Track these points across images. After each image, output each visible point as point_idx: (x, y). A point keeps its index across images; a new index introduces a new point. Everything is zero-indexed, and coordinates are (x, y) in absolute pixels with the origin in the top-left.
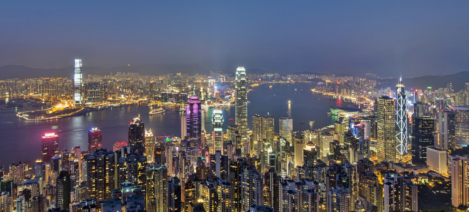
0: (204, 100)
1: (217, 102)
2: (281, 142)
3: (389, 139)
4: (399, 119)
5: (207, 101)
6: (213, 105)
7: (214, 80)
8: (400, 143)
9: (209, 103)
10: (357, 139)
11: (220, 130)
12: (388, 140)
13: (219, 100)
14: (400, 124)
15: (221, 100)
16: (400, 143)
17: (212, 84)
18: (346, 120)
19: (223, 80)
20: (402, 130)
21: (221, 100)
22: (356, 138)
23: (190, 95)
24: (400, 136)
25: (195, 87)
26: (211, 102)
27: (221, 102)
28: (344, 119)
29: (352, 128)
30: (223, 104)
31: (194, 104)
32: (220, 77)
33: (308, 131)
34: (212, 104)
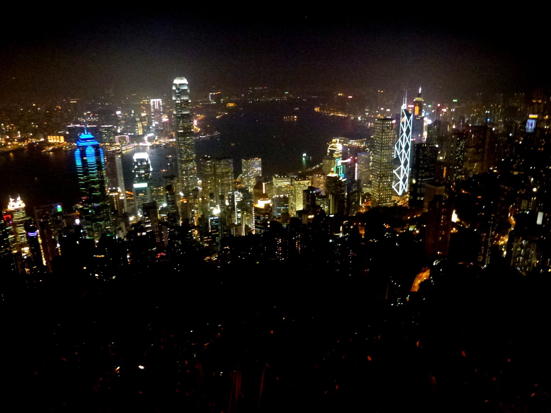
0: (143, 135)
1: (165, 136)
2: (236, 196)
3: (385, 177)
4: (401, 148)
6: (157, 143)
7: (158, 100)
8: (399, 180)
9: (150, 140)
10: (343, 180)
11: (144, 185)
12: (384, 178)
13: (170, 132)
14: (401, 155)
16: (399, 180)
17: (157, 107)
18: (338, 154)
20: (402, 162)
21: (172, 133)
22: (341, 181)
23: (121, 128)
24: (400, 169)
25: (133, 113)
26: (156, 137)
28: (335, 153)
29: (338, 165)
33: (277, 175)
34: (157, 141)
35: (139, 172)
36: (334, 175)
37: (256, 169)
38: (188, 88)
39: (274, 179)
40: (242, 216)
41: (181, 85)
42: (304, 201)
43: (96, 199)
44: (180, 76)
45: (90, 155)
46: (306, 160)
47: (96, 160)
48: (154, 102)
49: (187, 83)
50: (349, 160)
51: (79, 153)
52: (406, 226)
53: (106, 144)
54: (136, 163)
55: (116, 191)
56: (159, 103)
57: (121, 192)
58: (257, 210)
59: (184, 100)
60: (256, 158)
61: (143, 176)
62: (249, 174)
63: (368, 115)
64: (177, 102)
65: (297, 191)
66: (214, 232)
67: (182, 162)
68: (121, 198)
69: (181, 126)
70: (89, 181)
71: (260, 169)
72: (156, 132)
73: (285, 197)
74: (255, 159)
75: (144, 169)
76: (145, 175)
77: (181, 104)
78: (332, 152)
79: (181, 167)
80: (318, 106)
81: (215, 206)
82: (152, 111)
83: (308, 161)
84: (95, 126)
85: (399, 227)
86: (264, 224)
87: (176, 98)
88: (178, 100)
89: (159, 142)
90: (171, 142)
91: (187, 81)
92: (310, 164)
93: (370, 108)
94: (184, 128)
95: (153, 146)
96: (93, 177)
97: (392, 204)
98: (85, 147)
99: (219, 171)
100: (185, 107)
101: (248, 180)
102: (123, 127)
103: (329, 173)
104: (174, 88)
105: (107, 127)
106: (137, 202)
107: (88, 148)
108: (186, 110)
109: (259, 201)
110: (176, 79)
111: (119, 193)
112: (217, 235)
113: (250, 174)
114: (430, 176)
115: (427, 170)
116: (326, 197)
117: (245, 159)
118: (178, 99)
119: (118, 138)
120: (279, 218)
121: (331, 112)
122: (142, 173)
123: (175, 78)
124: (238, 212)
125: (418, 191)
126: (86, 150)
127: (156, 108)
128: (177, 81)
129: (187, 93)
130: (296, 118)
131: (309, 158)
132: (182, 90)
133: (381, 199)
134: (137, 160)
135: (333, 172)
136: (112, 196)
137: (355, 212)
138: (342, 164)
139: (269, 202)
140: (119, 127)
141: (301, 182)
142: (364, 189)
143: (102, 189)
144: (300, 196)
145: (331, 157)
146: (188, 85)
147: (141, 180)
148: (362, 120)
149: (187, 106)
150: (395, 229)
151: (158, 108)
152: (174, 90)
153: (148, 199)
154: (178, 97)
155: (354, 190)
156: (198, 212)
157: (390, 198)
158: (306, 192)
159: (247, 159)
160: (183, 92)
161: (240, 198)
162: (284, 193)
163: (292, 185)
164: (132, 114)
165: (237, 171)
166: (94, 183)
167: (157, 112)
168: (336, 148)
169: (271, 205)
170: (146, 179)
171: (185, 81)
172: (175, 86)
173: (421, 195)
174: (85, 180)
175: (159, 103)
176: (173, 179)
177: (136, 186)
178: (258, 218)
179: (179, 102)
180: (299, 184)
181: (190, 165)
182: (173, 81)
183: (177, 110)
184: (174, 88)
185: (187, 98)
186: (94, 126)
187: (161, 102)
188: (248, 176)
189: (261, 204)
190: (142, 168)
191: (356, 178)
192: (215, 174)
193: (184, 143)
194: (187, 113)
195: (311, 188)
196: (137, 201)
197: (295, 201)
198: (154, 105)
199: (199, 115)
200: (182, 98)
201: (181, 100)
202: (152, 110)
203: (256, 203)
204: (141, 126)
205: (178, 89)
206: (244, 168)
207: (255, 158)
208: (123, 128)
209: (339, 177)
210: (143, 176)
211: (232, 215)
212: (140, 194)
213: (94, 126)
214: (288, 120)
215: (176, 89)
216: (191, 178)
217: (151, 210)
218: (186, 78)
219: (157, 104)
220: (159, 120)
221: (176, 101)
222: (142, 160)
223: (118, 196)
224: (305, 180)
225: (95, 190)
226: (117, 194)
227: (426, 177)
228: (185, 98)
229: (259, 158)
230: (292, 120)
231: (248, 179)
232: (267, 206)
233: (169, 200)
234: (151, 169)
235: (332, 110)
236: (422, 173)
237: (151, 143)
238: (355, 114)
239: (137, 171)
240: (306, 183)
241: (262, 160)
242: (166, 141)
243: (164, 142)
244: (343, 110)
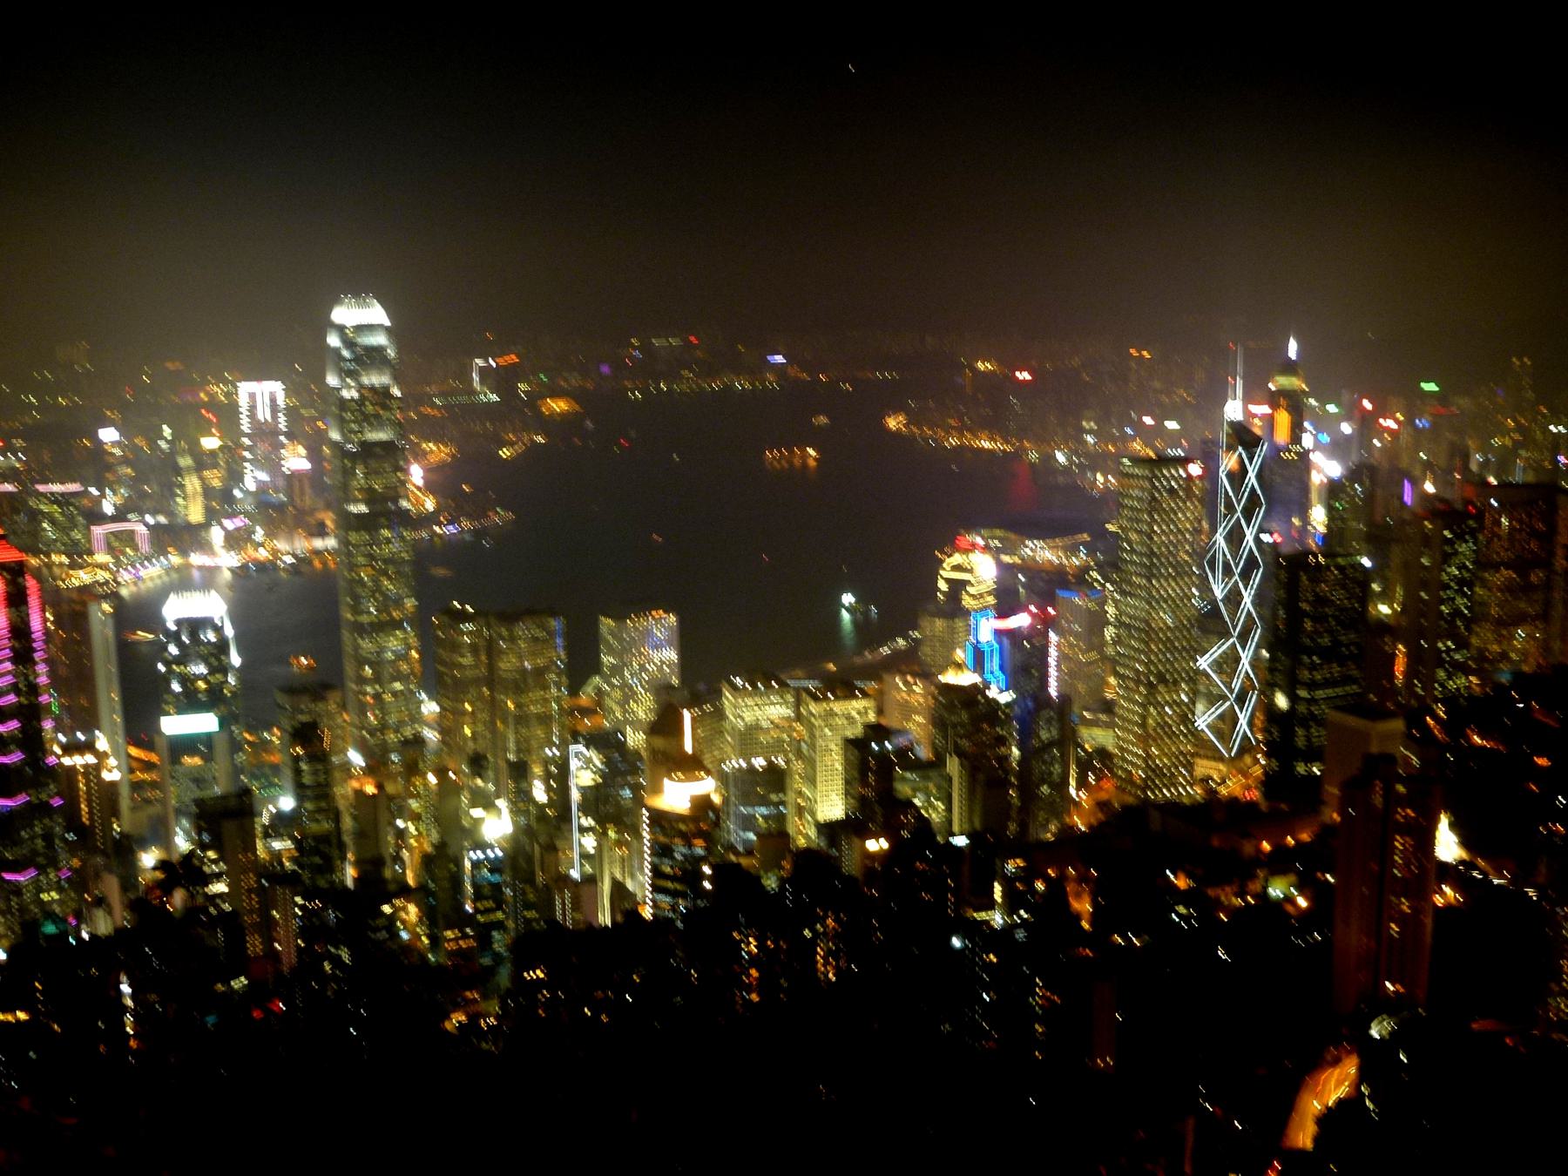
0: (206, 526)
2: (574, 764)
6: (263, 554)
9: (235, 541)
11: (205, 723)
13: (312, 511)
17: (264, 414)
36: (966, 678)
37: (656, 656)
39: (727, 694)
40: (599, 848)
41: (360, 329)
42: (847, 782)
46: (855, 622)
48: (252, 396)
49: (387, 323)
50: (1021, 621)
52: (1254, 877)
53: (55, 558)
54: (175, 637)
55: (89, 747)
56: (273, 401)
57: (109, 752)
58: (660, 819)
59: (372, 389)
65: (820, 742)
66: (487, 911)
67: (360, 629)
68: (107, 776)
71: (671, 655)
73: (771, 768)
77: (361, 402)
78: (957, 587)
79: (357, 648)
80: (896, 410)
81: (489, 805)
83: (861, 625)
85: (1229, 883)
86: (690, 875)
90: (317, 553)
92: (869, 633)
94: (371, 497)
97: (1198, 792)
99: (507, 664)
101: (623, 703)
103: (943, 670)
109: (666, 781)
111: (101, 756)
112: (500, 925)
114: (1346, 680)
115: (1329, 655)
116: (938, 763)
120: (749, 852)
124: (583, 830)
125: (1301, 742)
127: (260, 417)
128: (346, 314)
131: (867, 613)
133: (1154, 771)
134: (179, 622)
135: (959, 666)
136: (73, 769)
137: (1053, 828)
138: (998, 633)
139: (706, 786)
141: (838, 707)
142: (1084, 733)
143: (32, 742)
144: (833, 763)
145: (954, 608)
147: (190, 702)
150: (1211, 892)
154: (351, 374)
155: (1044, 735)
157: (1190, 767)
158: (856, 747)
159: (620, 617)
160: (372, 357)
162: (766, 751)
163: (799, 717)
165: (582, 664)
167: (264, 433)
168: (970, 571)
169: (717, 799)
170: (212, 700)
171: (376, 314)
173: (1311, 755)
175: (273, 401)
177: (174, 725)
178: (662, 851)
180: (831, 714)
183: (342, 424)
184: (333, 340)
188: (625, 686)
189: (676, 796)
191: (1053, 691)
192: (492, 680)
193: (371, 557)
195: (878, 731)
197: (812, 781)
200: (365, 380)
203: (657, 789)
205: (350, 344)
206: (611, 651)
209: (987, 685)
211: (559, 844)
216: (395, 694)
217: (229, 827)
220: (273, 464)
222: (194, 626)
223: (97, 768)
224: (850, 695)
226: (90, 759)
227: (1327, 684)
228: (376, 379)
232: (702, 805)
234: (235, 659)
236: (1313, 667)
238: (1045, 441)
240: (857, 711)
241: (681, 621)
244: (994, 426)
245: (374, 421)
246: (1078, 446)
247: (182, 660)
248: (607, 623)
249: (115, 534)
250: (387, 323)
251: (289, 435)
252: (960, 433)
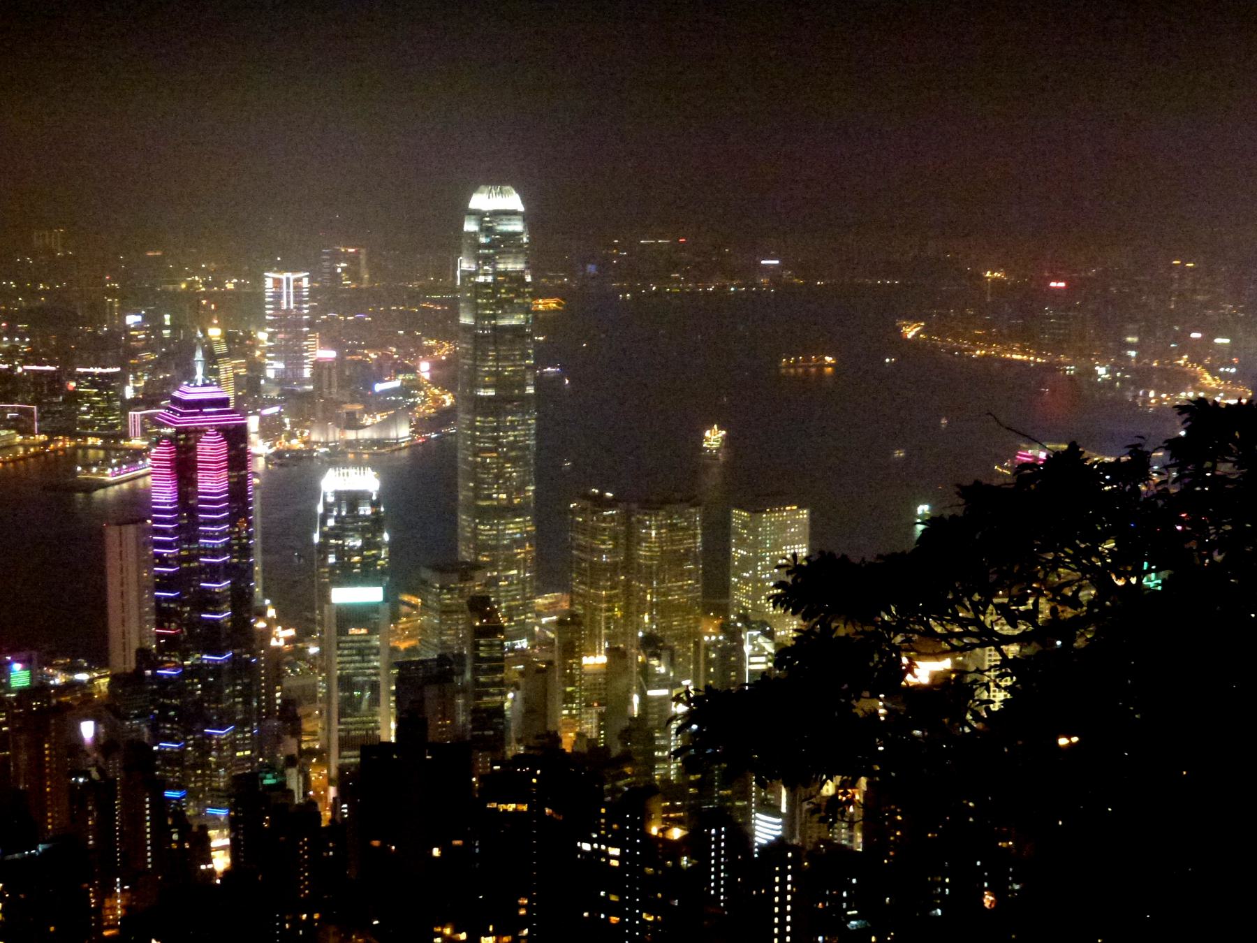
1: (326, 419)
2: (747, 648)
5: (255, 413)
6: (296, 444)
11: (371, 595)
13: (339, 404)
15: (349, 407)
19: (354, 274)
21: (349, 407)
23: (137, 379)
25: (167, 323)
27: (352, 422)
30: (364, 434)
31: (199, 431)
32: (337, 257)
34: (292, 435)
35: (340, 542)
38: (524, 227)
43: (211, 639)
44: (496, 179)
45: (213, 466)
47: (229, 483)
48: (278, 282)
49: (521, 208)
51: (167, 456)
53: (90, 441)
56: (298, 288)
59: (505, 273)
60: (788, 508)
61: (356, 559)
62: (759, 568)
63: (1138, 358)
64: (481, 279)
67: (485, 514)
69: (489, 374)
70: (196, 564)
72: (285, 401)
74: (785, 510)
75: (362, 532)
76: (364, 558)
77: (496, 286)
79: (475, 532)
80: (913, 319)
82: (267, 317)
84: (53, 368)
87: (478, 264)
88: (485, 274)
89: (305, 443)
90: (349, 444)
91: (523, 202)
93: (1145, 333)
94: (499, 382)
95: (279, 454)
96: (213, 550)
98: (195, 434)
100: (510, 301)
102: (146, 378)
104: (470, 226)
105: (100, 375)
106: (339, 659)
107: (204, 438)
108: (514, 311)
110: (482, 193)
113: (765, 568)
117: (741, 507)
118: (486, 268)
119: (138, 420)
121: (975, 341)
122: (351, 549)
123: (475, 189)
126: (199, 447)
127: (285, 307)
128: (482, 201)
129: (521, 246)
130: (830, 365)
132: (503, 234)
134: (339, 495)
140: (131, 377)
143: (242, 602)
146: (526, 217)
147: (346, 575)
148: (1115, 379)
149: (518, 296)
151: (292, 306)
152: (469, 233)
153: (381, 651)
154: (487, 259)
156: (574, 712)
160: (506, 243)
161: (763, 659)
164: (167, 327)
166: (214, 573)
167: (286, 322)
170: (367, 575)
171: (512, 201)
172: (473, 217)
174: (180, 559)
175: (298, 288)
176: (472, 579)
177: (342, 596)
179: (490, 279)
181: (514, 528)
182: (468, 201)
184: (470, 226)
185: (520, 266)
186: (48, 368)
187: (305, 283)
188: (755, 579)
190: (355, 530)
192: (629, 565)
194: (514, 322)
196: (341, 655)
198: (277, 296)
199: (433, 343)
200: (501, 267)
201: (496, 273)
202: (268, 312)
204: (231, 375)
205: (488, 231)
206: (742, 543)
207: (786, 505)
208: (147, 384)
210: (356, 559)
212: (353, 631)
213: (48, 368)
214: (800, 370)
215: (481, 230)
218: (518, 191)
219: (292, 290)
220: (293, 355)
221: (476, 274)
222: (352, 499)
225: (208, 601)
228: (513, 265)
229: (800, 507)
230: (813, 370)
231: (754, 587)
233: (481, 654)
235: (979, 338)
237: (268, 444)
238: (1084, 355)
239: (333, 541)
241: (811, 514)
242: (331, 438)
243: (322, 440)
244: (1026, 337)
245: (505, 306)
246: (1119, 363)
247: (339, 532)
248: (739, 516)
249: (146, 416)
250: (521, 208)
251: (310, 324)
252: (988, 341)
